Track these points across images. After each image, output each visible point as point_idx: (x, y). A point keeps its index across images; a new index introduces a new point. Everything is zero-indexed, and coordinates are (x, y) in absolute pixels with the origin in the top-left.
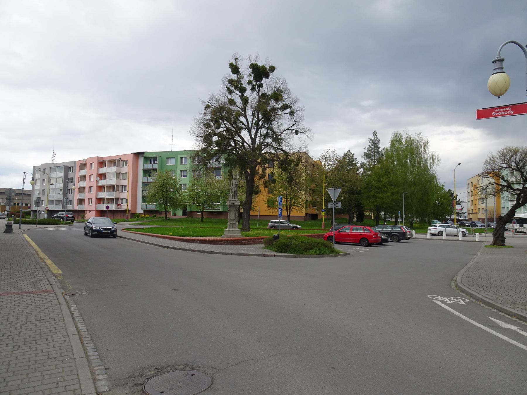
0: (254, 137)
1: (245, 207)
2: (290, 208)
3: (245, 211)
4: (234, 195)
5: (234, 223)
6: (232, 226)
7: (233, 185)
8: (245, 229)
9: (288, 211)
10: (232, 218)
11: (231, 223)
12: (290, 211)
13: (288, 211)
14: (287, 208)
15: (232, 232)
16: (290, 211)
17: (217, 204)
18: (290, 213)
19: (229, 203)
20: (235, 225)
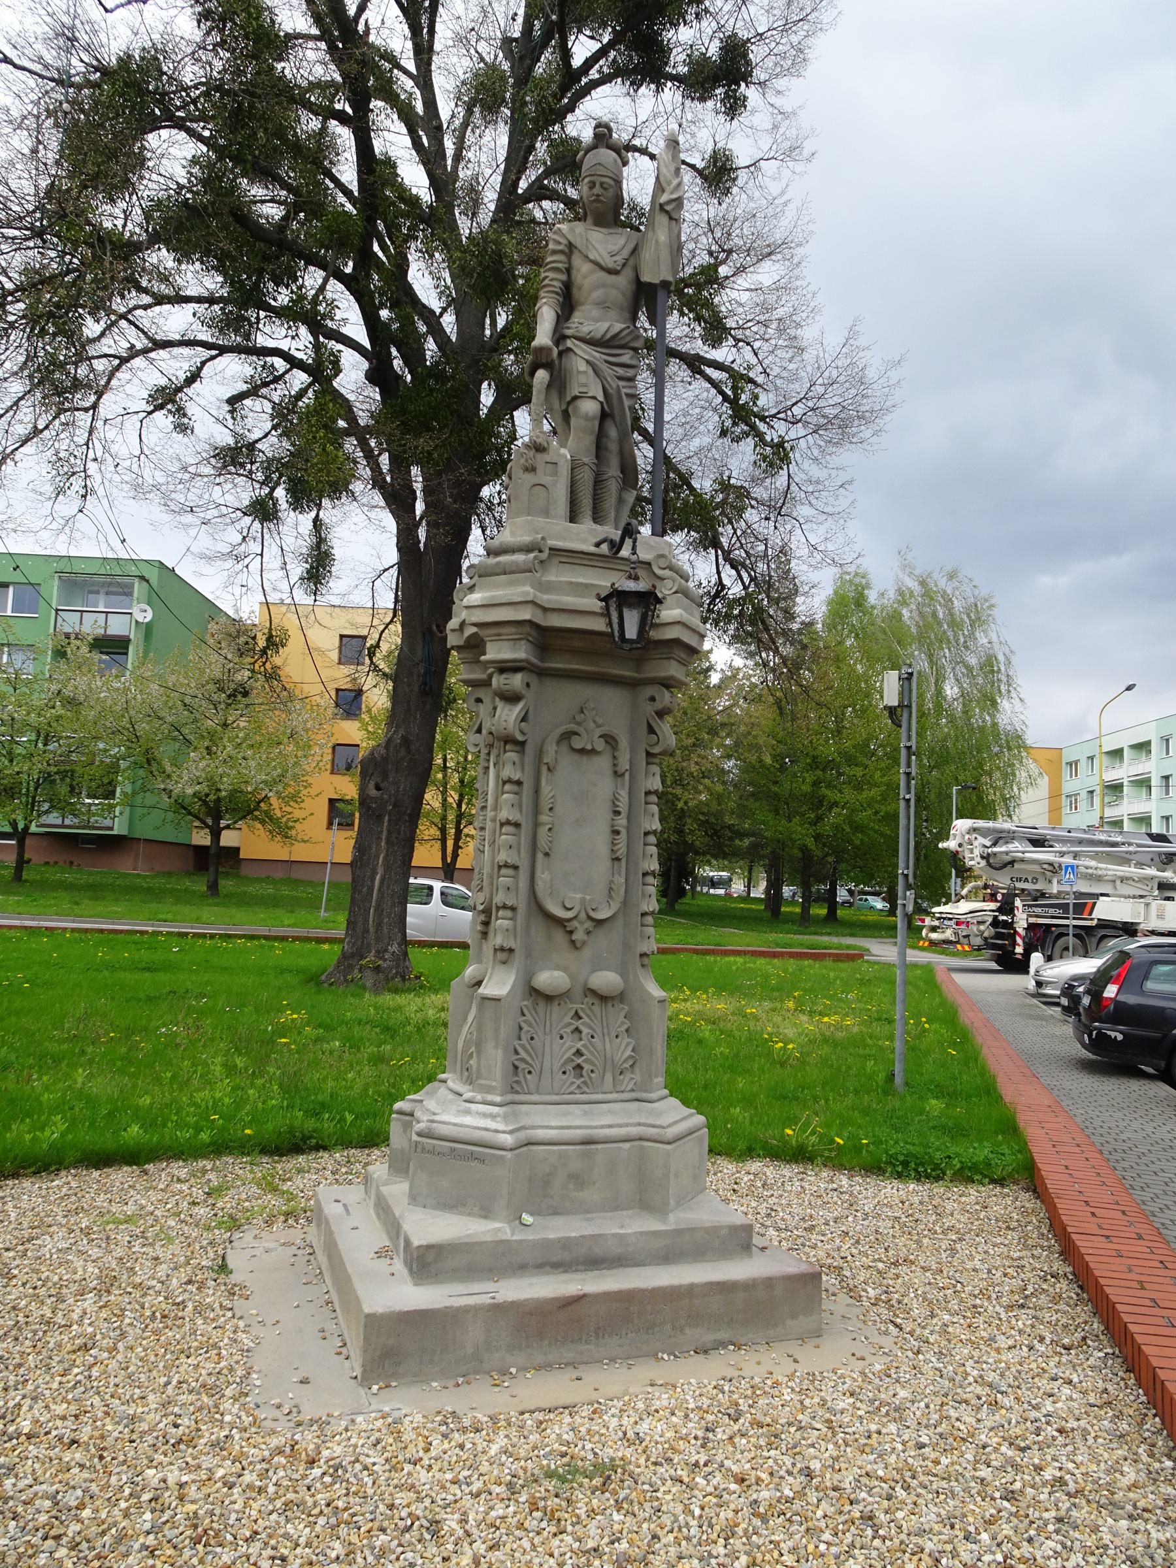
0: (525, 191)
1: (378, 788)
2: (459, 832)
3: (380, 818)
4: (598, 482)
5: (607, 979)
6: (559, 1050)
7: (568, 304)
8: (378, 969)
9: (450, 844)
10: (574, 898)
11: (549, 978)
12: (457, 847)
13: (450, 844)
14: (443, 830)
15: (578, 1180)
16: (457, 847)
17: (418, 487)
18: (455, 855)
19: (524, 590)
20: (617, 1018)
